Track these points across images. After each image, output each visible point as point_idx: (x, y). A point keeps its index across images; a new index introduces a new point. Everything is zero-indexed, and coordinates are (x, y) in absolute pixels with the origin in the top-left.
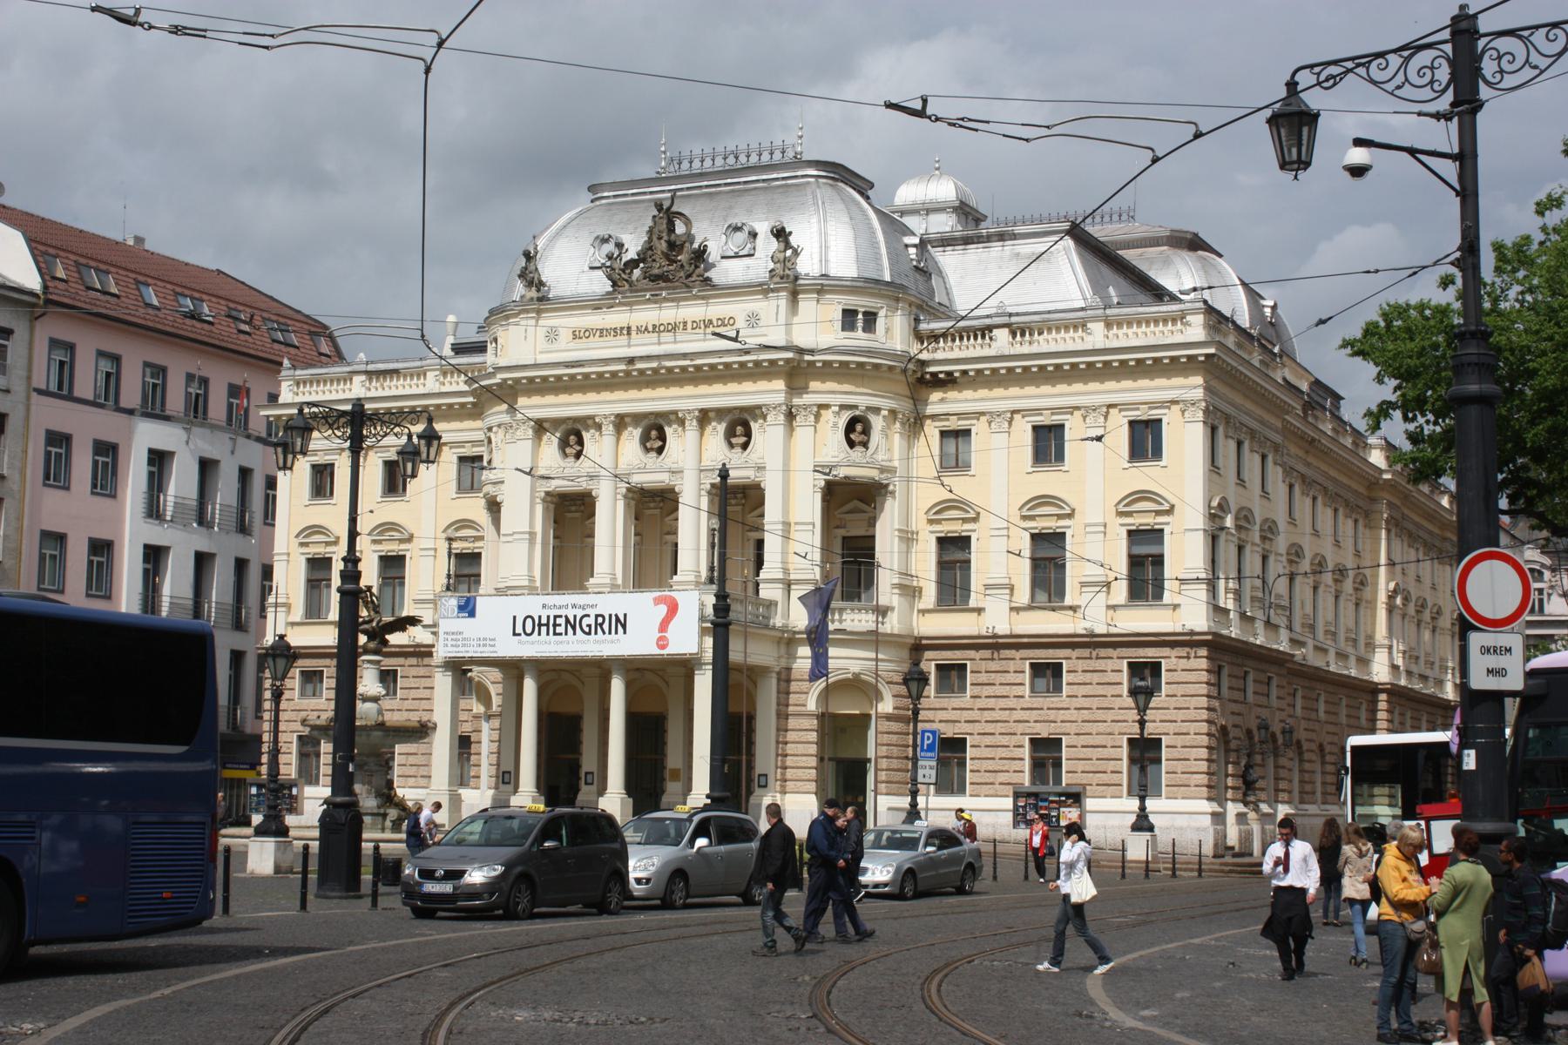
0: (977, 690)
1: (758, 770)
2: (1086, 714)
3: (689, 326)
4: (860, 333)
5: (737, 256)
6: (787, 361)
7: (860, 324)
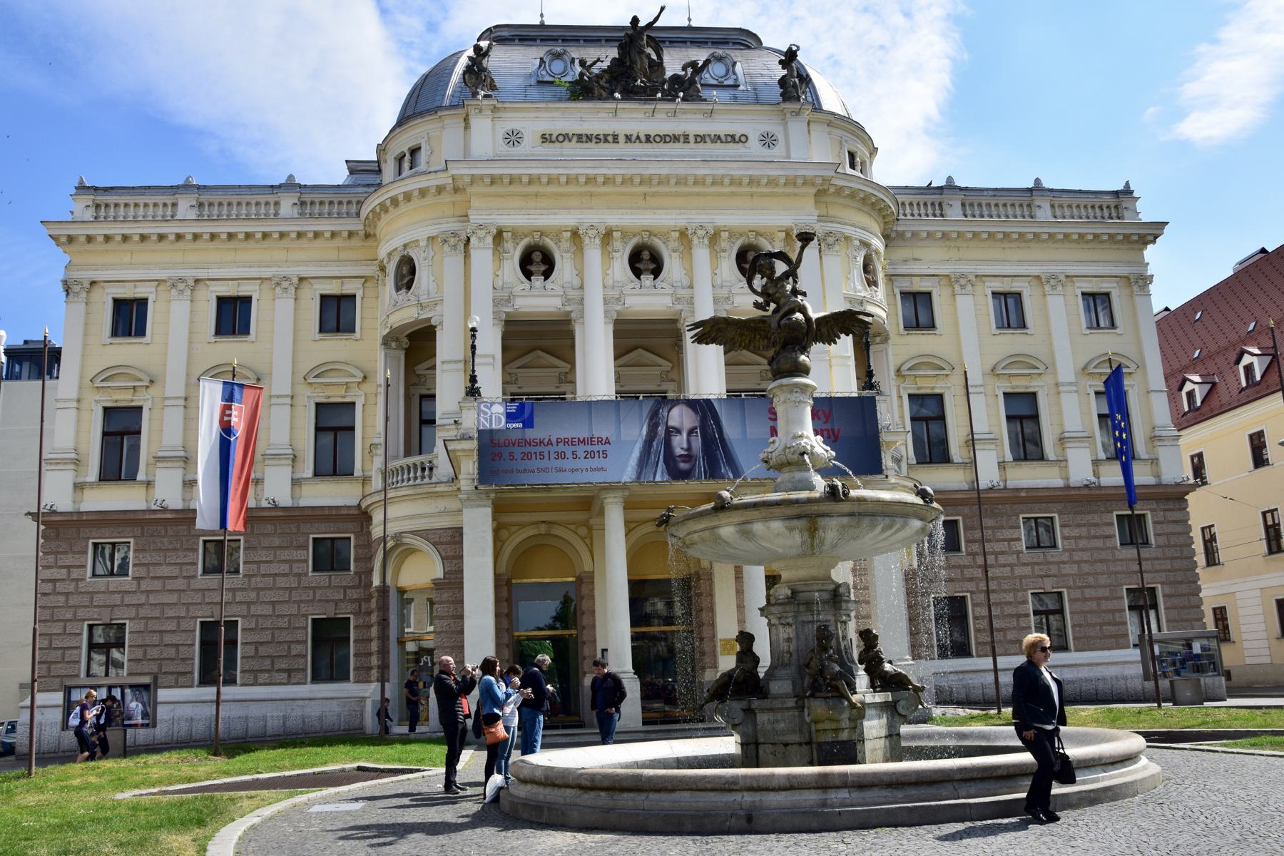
2: (1086, 568)
3: (692, 139)
4: (858, 174)
5: (720, 86)
6: (824, 179)
7: (859, 167)
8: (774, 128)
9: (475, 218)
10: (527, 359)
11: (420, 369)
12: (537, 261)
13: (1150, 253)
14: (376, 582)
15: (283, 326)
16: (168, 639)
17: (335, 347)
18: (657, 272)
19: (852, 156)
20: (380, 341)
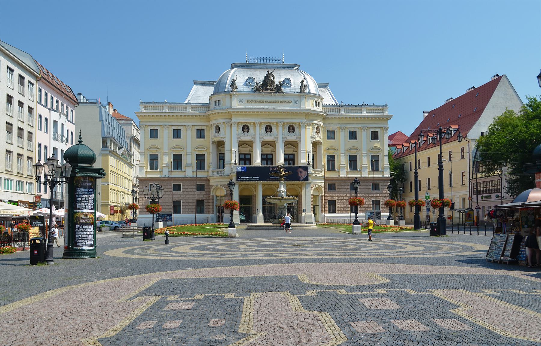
0: (339, 190)
1: (304, 207)
5: (287, 86)
8: (298, 99)
9: (233, 120)
10: (242, 146)
11: (219, 148)
12: (246, 128)
13: (389, 122)
14: (211, 194)
15: (188, 135)
16: (167, 204)
17: (200, 142)
18: (271, 132)
19: (316, 102)
20: (211, 143)
